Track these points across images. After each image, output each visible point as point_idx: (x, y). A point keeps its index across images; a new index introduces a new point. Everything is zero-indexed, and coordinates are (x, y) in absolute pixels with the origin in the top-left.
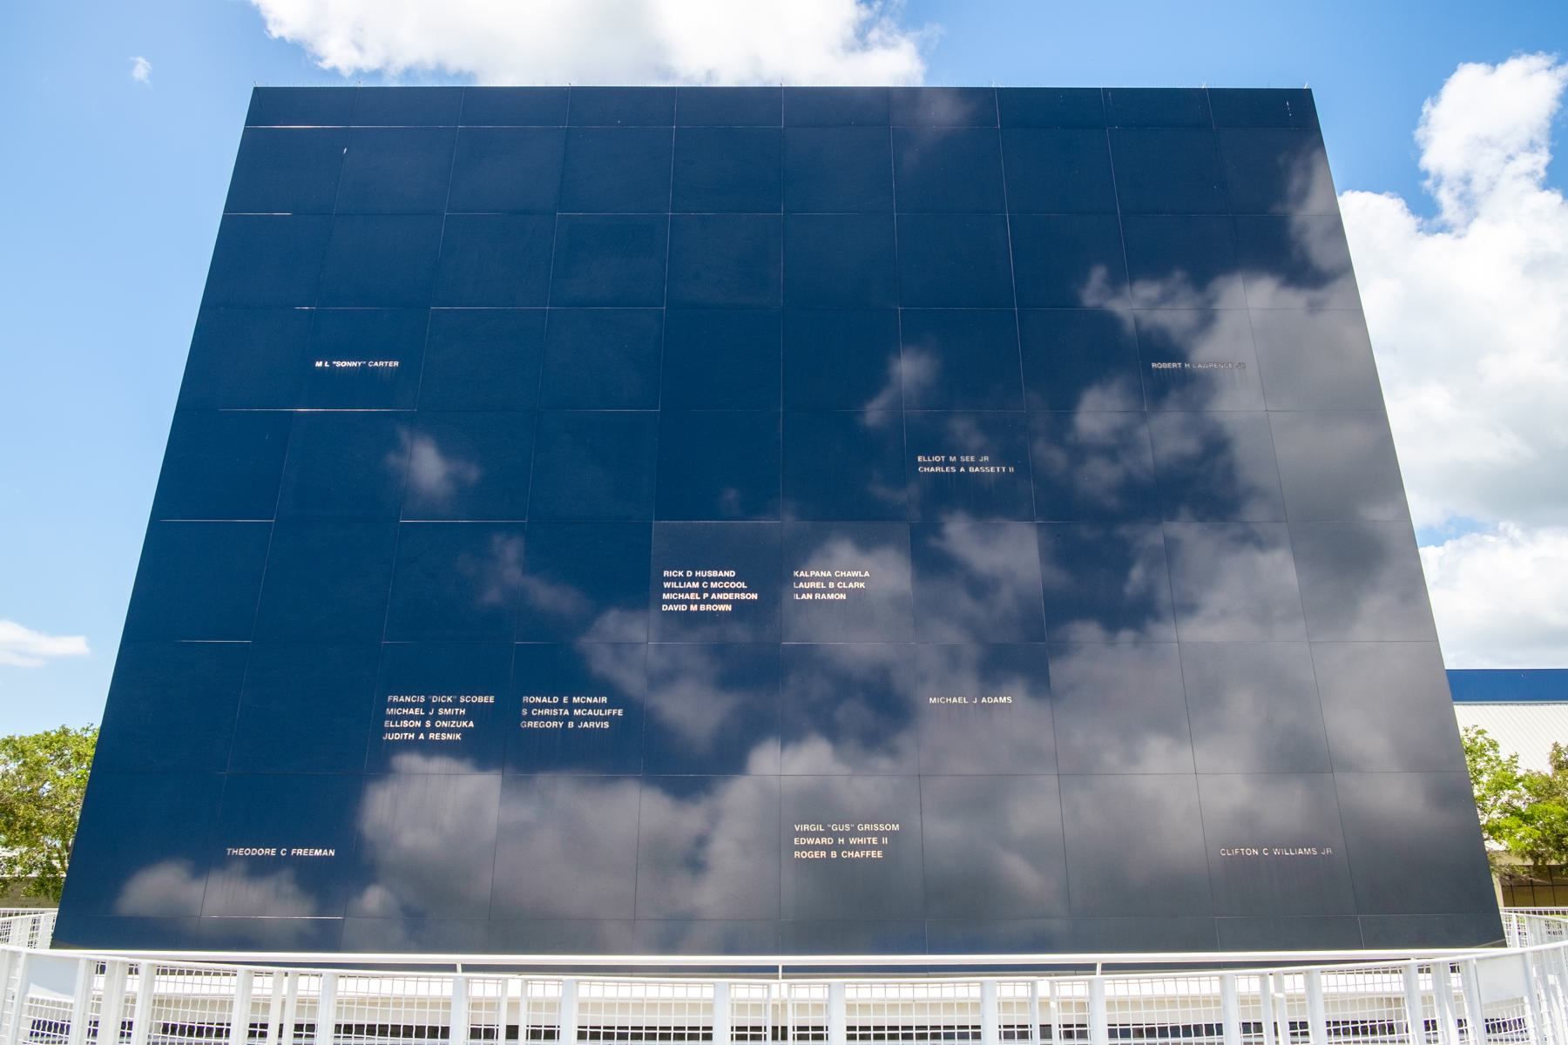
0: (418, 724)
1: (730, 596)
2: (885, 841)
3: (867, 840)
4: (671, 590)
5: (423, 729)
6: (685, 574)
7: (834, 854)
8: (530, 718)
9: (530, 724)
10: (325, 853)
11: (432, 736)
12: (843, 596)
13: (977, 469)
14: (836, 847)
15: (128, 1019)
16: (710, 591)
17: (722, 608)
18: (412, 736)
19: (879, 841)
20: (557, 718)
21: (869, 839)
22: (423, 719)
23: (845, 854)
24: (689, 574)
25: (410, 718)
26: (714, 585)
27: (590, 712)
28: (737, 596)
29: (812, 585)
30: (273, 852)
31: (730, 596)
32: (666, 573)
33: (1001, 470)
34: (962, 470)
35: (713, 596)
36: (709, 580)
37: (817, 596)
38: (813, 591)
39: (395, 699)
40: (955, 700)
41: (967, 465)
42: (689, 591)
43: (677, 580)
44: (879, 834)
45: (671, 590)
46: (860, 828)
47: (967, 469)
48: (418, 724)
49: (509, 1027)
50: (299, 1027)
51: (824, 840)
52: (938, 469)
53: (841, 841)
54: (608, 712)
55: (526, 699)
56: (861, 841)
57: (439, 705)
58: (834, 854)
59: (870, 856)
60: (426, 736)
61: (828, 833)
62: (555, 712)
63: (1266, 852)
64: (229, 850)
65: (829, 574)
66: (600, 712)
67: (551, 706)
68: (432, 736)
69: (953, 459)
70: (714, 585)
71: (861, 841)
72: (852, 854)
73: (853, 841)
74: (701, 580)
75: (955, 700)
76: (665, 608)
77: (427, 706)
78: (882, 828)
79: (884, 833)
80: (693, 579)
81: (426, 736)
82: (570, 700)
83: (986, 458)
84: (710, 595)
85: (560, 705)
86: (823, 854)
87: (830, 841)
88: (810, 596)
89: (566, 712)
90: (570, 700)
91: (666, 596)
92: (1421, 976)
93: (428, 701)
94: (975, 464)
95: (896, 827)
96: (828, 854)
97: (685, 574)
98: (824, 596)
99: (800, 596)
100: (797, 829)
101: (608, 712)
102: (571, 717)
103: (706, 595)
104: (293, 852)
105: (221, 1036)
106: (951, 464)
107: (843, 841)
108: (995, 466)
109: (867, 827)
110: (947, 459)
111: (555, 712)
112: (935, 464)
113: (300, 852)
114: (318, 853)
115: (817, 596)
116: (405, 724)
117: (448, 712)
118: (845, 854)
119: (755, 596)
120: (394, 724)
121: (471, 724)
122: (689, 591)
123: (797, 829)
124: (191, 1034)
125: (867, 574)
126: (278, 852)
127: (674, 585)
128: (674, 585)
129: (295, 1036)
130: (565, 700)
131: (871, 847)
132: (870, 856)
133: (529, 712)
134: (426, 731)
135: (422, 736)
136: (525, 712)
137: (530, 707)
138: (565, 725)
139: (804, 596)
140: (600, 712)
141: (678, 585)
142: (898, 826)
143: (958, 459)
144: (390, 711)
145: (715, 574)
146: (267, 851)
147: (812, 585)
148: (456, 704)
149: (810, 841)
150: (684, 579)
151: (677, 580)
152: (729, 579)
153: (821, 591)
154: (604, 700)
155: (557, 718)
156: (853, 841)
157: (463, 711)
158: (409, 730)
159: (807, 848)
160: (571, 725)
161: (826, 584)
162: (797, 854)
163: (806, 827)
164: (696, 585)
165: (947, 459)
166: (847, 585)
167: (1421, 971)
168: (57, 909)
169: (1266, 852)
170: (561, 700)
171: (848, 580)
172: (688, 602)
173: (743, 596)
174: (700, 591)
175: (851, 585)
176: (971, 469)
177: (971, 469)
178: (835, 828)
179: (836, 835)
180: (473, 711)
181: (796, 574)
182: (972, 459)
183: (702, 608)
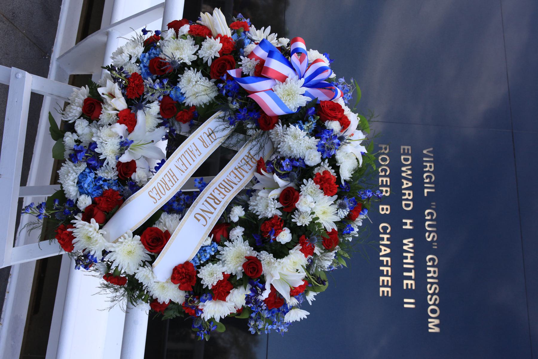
2: (409, 303)
3: (409, 270)
19: (409, 293)
21: (412, 274)
23: (385, 228)
51: (408, 195)
53: (408, 224)
56: (408, 261)
59: (382, 273)
71: (408, 261)
72: (386, 242)
73: (408, 244)
78: (432, 301)
79: (422, 304)
86: (386, 192)
87: (407, 205)
100: (425, 152)
107: (408, 227)
109: (432, 272)
123: (425, 152)
132: (382, 273)
142: (437, 330)
149: (406, 172)
156: (408, 244)
163: (429, 167)
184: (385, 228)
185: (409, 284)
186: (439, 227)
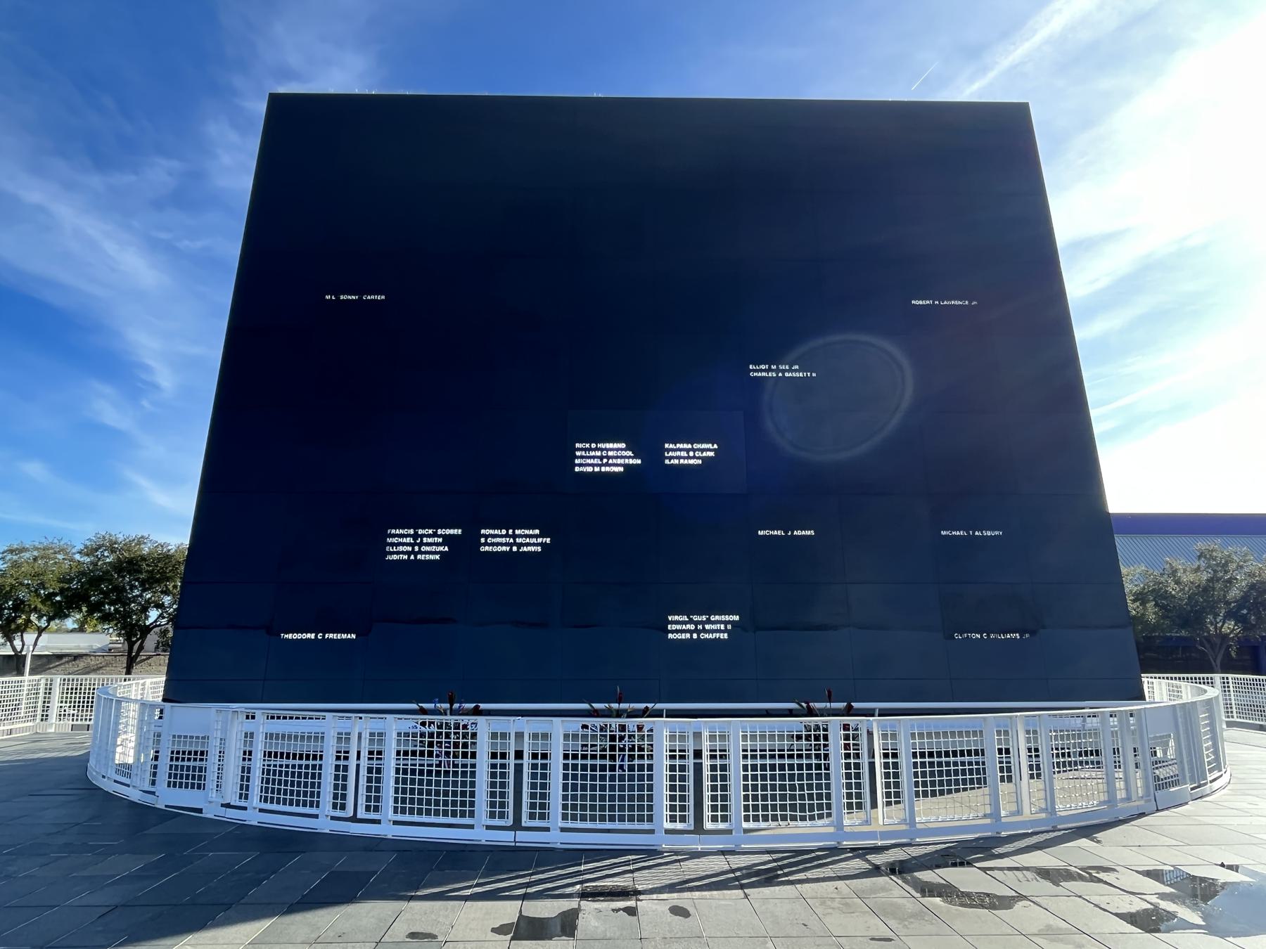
0: (410, 549)
1: (619, 461)
2: (729, 627)
4: (582, 457)
5: (413, 552)
6: (590, 446)
7: (695, 636)
8: (486, 544)
9: (487, 548)
10: (349, 636)
11: (419, 557)
12: (700, 462)
13: (790, 375)
14: (696, 631)
15: (248, 749)
16: (608, 458)
18: (406, 557)
19: (726, 627)
20: (506, 544)
22: (412, 545)
24: (593, 446)
25: (403, 544)
27: (528, 540)
28: (627, 461)
29: (678, 453)
30: (313, 636)
31: (619, 461)
32: (577, 445)
33: (807, 375)
34: (780, 375)
35: (610, 461)
37: (682, 461)
38: (679, 458)
39: (393, 531)
40: (776, 533)
41: (783, 371)
42: (594, 457)
43: (585, 450)
44: (726, 623)
45: (582, 457)
46: (713, 618)
47: (783, 374)
48: (410, 549)
49: (516, 752)
50: (371, 753)
52: (764, 374)
54: (540, 540)
55: (483, 531)
57: (422, 536)
58: (695, 636)
59: (719, 637)
60: (416, 557)
61: (691, 621)
62: (503, 540)
64: (282, 635)
65: (690, 446)
66: (534, 540)
67: (501, 536)
68: (419, 557)
69: (774, 367)
70: (610, 453)
73: (707, 627)
74: (602, 450)
75: (776, 533)
76: (577, 469)
77: (415, 536)
78: (727, 618)
79: (729, 622)
80: (597, 449)
81: (416, 557)
82: (514, 532)
83: (797, 367)
84: (608, 460)
85: (507, 536)
86: (688, 636)
88: (676, 462)
89: (512, 540)
90: (514, 532)
91: (577, 461)
92: (1111, 719)
93: (416, 533)
94: (790, 371)
95: (737, 618)
96: (691, 636)
97: (590, 446)
98: (686, 462)
99: (670, 461)
101: (540, 540)
102: (515, 544)
103: (605, 461)
104: (326, 636)
105: (933, 757)
106: (773, 371)
108: (803, 372)
110: (770, 367)
111: (503, 540)
112: (761, 371)
113: (331, 636)
114: (344, 636)
115: (682, 461)
116: (401, 548)
117: (430, 540)
118: (703, 636)
119: (639, 462)
120: (393, 549)
121: (446, 549)
122: (594, 457)
124: (294, 758)
125: (716, 446)
126: (316, 636)
127: (583, 453)
128: (583, 453)
129: (369, 759)
130: (510, 532)
132: (719, 637)
133: (486, 540)
134: (416, 554)
135: (412, 557)
136: (483, 540)
137: (486, 537)
138: (511, 549)
139: (672, 462)
140: (534, 540)
141: (586, 453)
142: (738, 617)
143: (778, 367)
144: (389, 540)
146: (309, 636)
147: (678, 453)
148: (435, 535)
149: (679, 627)
150: (590, 449)
151: (585, 450)
152: (622, 450)
154: (537, 532)
155: (506, 544)
156: (707, 627)
157: (440, 540)
158: (403, 553)
159: (677, 631)
160: (515, 549)
161: (688, 453)
162: (670, 636)
164: (598, 454)
165: (770, 367)
166: (702, 453)
167: (1111, 716)
168: (164, 678)
170: (508, 532)
171: (703, 450)
173: (631, 461)
174: (601, 458)
175: (704, 454)
176: (787, 375)
177: (787, 375)
178: (696, 618)
179: (696, 623)
180: (447, 540)
182: (787, 368)
183: (603, 469)
184: (703, 636)
185: (722, 627)
186: (700, 614)
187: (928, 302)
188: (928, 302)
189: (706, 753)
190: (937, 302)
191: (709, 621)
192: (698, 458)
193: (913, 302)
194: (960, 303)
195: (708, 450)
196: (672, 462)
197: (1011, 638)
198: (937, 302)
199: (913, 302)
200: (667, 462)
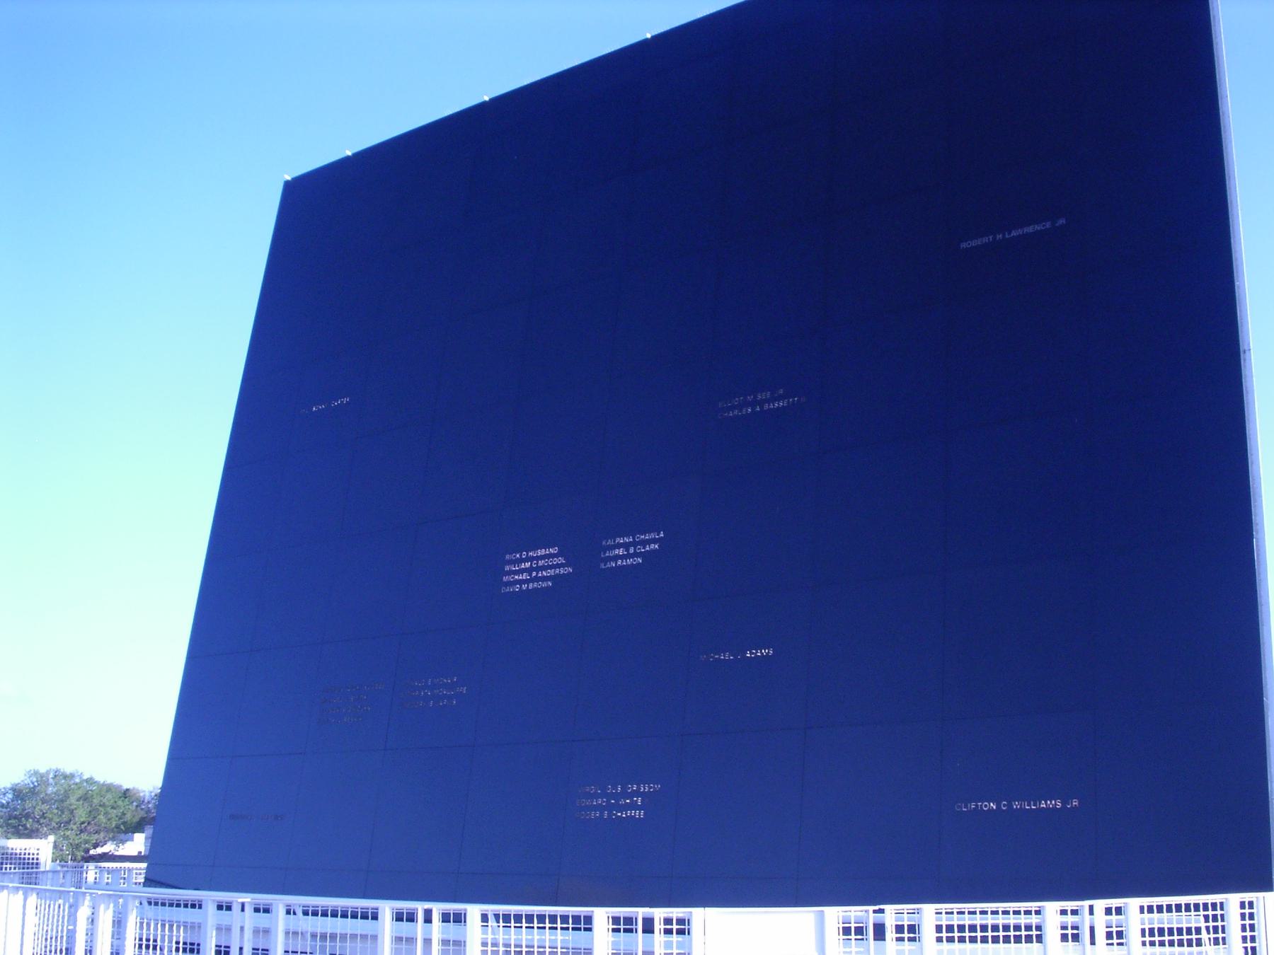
1: (551, 572)
14: (610, 807)
17: (544, 585)
26: (541, 563)
31: (551, 572)
32: (508, 557)
36: (539, 558)
37: (619, 562)
41: (761, 403)
44: (643, 795)
52: (736, 412)
63: (1004, 805)
69: (750, 398)
70: (541, 563)
84: (537, 574)
94: (768, 401)
96: (602, 814)
103: (534, 574)
106: (747, 404)
112: (733, 408)
131: (633, 806)
145: (541, 552)
153: (622, 557)
161: (627, 550)
164: (528, 565)
169: (1004, 805)
171: (644, 543)
172: (521, 582)
174: (529, 570)
176: (766, 407)
181: (604, 543)
183: (531, 586)
187: (985, 240)
188: (985, 240)
189: (144, 940)
190: (999, 237)
191: (625, 795)
192: (636, 555)
193: (964, 245)
194: (1038, 228)
195: (652, 542)
196: (619, 562)
197: (1048, 809)
198: (999, 237)
199: (964, 245)
200: (602, 566)
